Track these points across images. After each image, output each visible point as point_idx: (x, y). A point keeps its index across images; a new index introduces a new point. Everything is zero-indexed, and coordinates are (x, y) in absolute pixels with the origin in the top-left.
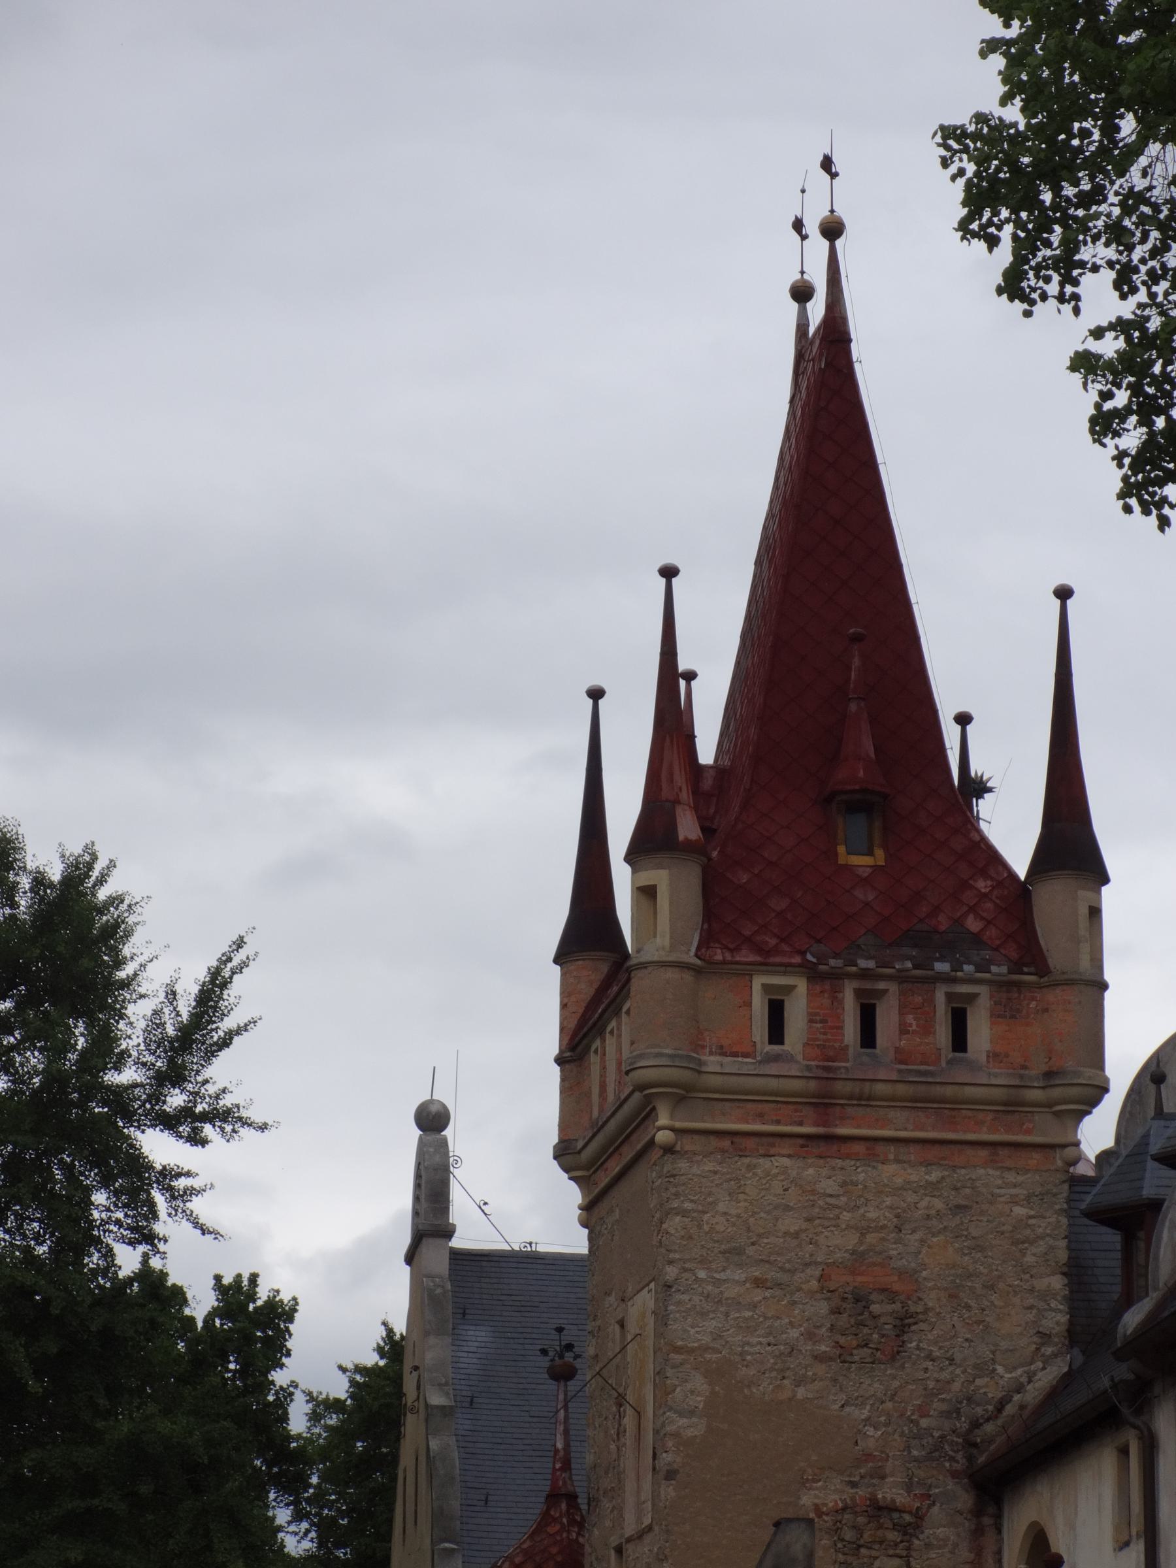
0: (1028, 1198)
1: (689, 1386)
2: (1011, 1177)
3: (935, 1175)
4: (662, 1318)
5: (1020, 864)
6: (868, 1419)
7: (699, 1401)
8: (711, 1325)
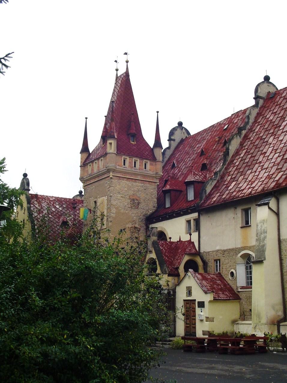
0: (153, 189)
1: (113, 210)
2: (151, 186)
3: (142, 185)
4: (109, 201)
5: (152, 147)
6: (134, 216)
7: (115, 212)
8: (116, 202)
